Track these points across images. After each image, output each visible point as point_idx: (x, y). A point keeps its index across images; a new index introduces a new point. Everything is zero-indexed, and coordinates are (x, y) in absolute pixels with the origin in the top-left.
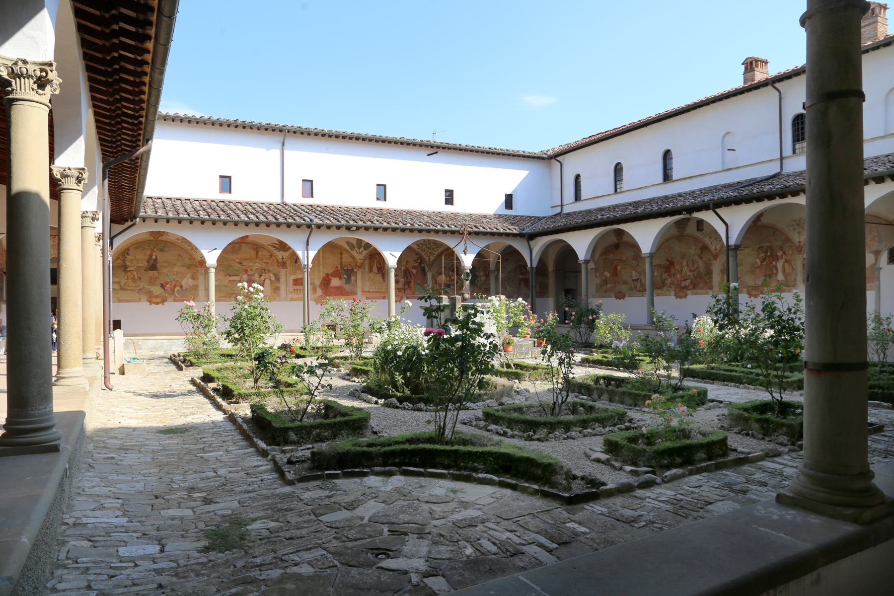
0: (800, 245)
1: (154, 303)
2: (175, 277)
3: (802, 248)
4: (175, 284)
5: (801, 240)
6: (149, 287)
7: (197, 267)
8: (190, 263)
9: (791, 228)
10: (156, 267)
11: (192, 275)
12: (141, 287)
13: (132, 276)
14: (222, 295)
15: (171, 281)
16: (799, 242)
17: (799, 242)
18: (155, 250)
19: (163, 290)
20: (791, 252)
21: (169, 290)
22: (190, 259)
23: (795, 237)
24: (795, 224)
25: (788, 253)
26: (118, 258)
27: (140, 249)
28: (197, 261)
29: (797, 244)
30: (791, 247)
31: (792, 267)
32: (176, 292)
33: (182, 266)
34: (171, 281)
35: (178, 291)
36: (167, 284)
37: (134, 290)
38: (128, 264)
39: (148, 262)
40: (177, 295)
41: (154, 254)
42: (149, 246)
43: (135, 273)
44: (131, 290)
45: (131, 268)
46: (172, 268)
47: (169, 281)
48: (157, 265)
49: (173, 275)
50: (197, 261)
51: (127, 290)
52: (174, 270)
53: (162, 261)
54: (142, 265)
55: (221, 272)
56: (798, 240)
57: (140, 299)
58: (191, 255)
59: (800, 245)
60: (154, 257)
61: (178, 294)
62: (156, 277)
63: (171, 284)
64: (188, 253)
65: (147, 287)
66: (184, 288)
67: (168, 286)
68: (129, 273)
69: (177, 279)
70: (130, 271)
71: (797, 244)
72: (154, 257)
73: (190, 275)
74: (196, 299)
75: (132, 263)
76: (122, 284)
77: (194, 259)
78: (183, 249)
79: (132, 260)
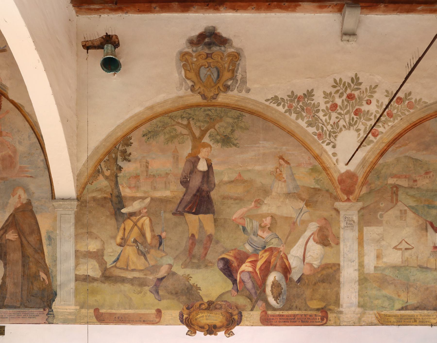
1: (202, 328)
2: (266, 235)
4: (268, 262)
6: (188, 271)
7: (336, 199)
8: (313, 185)
10: (209, 200)
11: (321, 229)
12: (162, 272)
13: (135, 233)
14: (413, 301)
15: (256, 253)
18: (206, 140)
19: (229, 285)
21: (249, 285)
22: (314, 170)
26: (97, 172)
27: (162, 138)
28: (336, 176)
32: (268, 290)
33: (288, 195)
34: (256, 253)
35: (276, 285)
36: (241, 262)
37: (142, 283)
38: (126, 192)
39: (185, 182)
40: (271, 300)
41: (203, 153)
42: (188, 126)
43: (145, 221)
44: (132, 281)
45: (134, 207)
46: (259, 203)
47: (248, 248)
48: (214, 195)
49: (262, 227)
50: (336, 176)
51: (123, 280)
52: (264, 209)
53: (226, 179)
54: (167, 193)
55: (410, 214)
57: (159, 311)
58: (317, 157)
60: (202, 166)
61: (276, 298)
62: (210, 237)
63: (254, 263)
64: (308, 149)
65: (180, 271)
66: (295, 276)
67: (246, 267)
68: (129, 224)
69: (274, 243)
70: (131, 214)
72: (202, 166)
73: (313, 227)
74: (331, 316)
75: (137, 187)
76: (109, 260)
77: (325, 169)
78: (291, 134)
79: (137, 177)
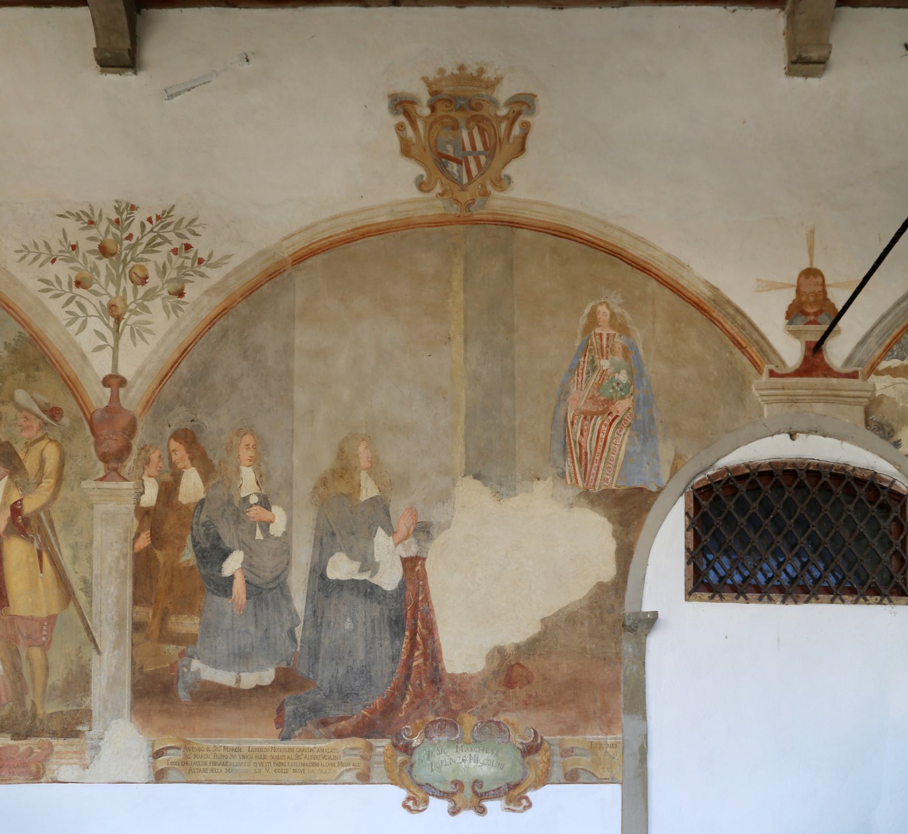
0: (113, 409)
3: (131, 429)
5: (126, 371)
9: (63, 271)
16: (115, 381)
17: (115, 381)
20: (51, 454)
23: (86, 340)
24: (85, 246)
25: (30, 463)
29: (99, 397)
30: (54, 413)
31: (62, 579)
56: (102, 366)
59: (113, 409)
71: (99, 397)
